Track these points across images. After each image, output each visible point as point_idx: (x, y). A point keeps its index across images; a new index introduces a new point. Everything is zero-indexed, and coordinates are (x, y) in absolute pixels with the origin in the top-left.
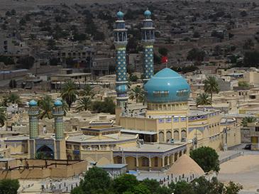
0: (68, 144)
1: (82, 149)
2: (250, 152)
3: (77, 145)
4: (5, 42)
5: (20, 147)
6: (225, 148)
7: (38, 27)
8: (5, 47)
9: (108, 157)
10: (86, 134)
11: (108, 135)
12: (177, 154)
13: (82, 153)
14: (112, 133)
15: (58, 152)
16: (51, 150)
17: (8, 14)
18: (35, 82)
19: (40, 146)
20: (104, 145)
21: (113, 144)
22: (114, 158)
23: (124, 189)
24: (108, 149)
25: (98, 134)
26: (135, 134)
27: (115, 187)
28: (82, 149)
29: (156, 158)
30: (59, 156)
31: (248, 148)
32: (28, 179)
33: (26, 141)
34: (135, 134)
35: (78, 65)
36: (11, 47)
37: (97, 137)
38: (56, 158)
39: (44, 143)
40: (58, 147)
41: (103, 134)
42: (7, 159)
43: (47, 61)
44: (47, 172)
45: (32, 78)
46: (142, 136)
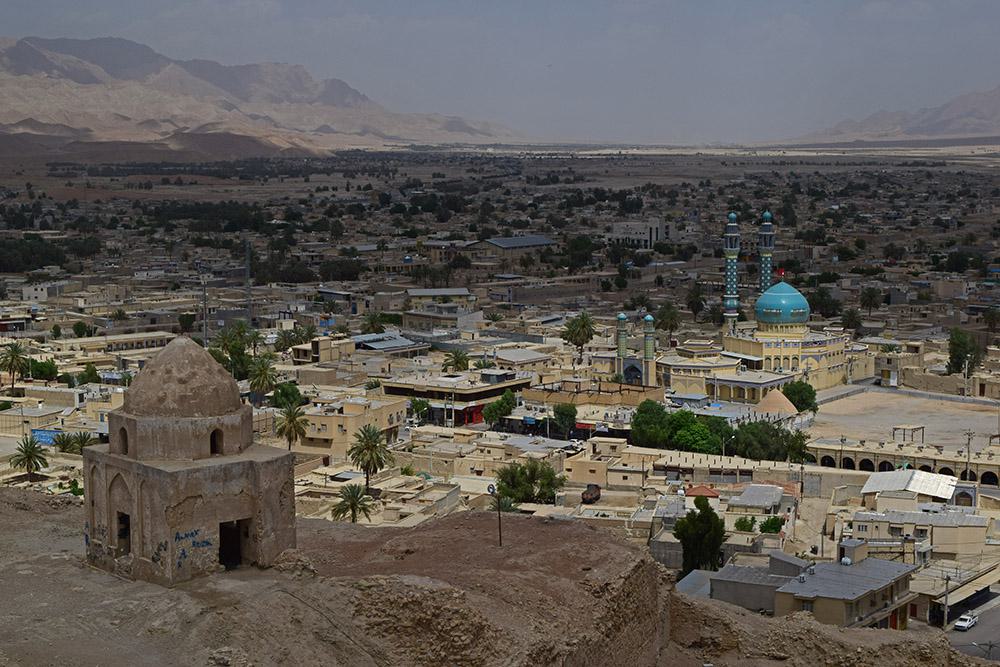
0: (659, 366)
1: (672, 372)
2: (881, 389)
3: (668, 367)
4: (667, 227)
5: (609, 364)
6: (850, 381)
7: (726, 205)
8: (667, 233)
9: (701, 386)
10: (680, 355)
11: (705, 359)
12: (773, 386)
13: (672, 377)
14: (710, 356)
15: (647, 374)
16: (637, 370)
17: (701, 185)
18: (682, 280)
19: (627, 366)
20: (697, 369)
21: (707, 370)
22: (707, 386)
23: (680, 427)
24: (702, 374)
25: (692, 357)
26: (738, 358)
27: (671, 423)
28: (672, 372)
29: (754, 389)
30: (647, 382)
31: (878, 383)
32: (595, 404)
33: (613, 358)
34: (738, 358)
35: (747, 258)
36: (673, 232)
37: (691, 360)
38: (644, 384)
39: (632, 362)
40: (647, 368)
41: (699, 356)
42: (581, 380)
43: (712, 251)
44: (617, 398)
45: (680, 275)
46: (744, 361)
